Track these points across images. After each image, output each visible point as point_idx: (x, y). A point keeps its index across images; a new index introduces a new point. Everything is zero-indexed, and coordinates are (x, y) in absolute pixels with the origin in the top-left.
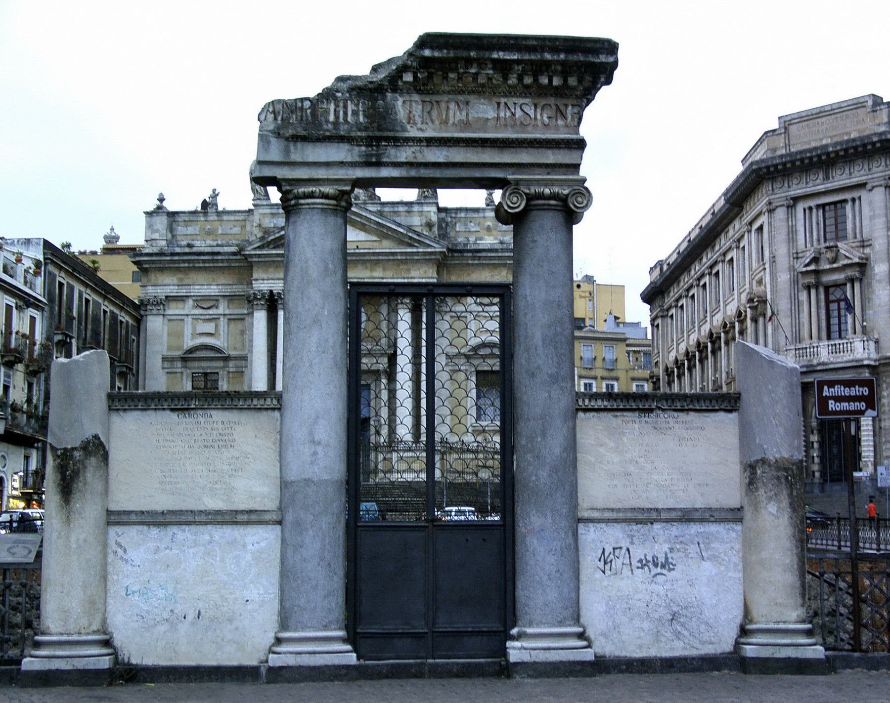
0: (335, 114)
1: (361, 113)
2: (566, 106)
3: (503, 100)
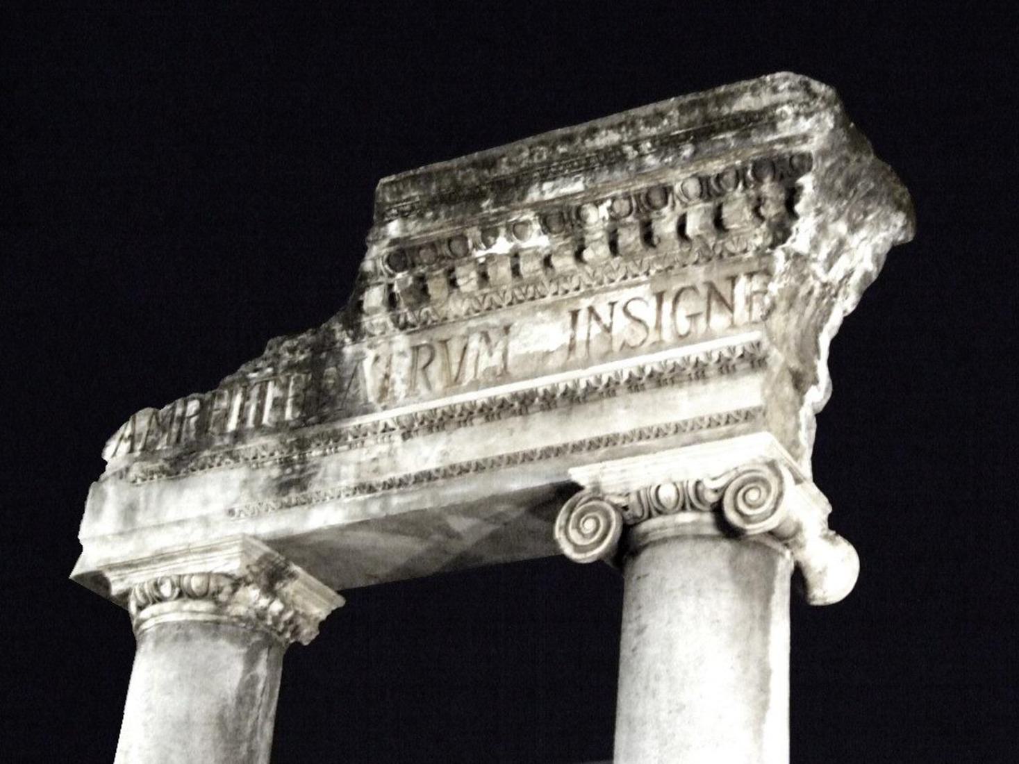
0: (239, 416)
1: (289, 401)
2: (733, 280)
3: (584, 303)
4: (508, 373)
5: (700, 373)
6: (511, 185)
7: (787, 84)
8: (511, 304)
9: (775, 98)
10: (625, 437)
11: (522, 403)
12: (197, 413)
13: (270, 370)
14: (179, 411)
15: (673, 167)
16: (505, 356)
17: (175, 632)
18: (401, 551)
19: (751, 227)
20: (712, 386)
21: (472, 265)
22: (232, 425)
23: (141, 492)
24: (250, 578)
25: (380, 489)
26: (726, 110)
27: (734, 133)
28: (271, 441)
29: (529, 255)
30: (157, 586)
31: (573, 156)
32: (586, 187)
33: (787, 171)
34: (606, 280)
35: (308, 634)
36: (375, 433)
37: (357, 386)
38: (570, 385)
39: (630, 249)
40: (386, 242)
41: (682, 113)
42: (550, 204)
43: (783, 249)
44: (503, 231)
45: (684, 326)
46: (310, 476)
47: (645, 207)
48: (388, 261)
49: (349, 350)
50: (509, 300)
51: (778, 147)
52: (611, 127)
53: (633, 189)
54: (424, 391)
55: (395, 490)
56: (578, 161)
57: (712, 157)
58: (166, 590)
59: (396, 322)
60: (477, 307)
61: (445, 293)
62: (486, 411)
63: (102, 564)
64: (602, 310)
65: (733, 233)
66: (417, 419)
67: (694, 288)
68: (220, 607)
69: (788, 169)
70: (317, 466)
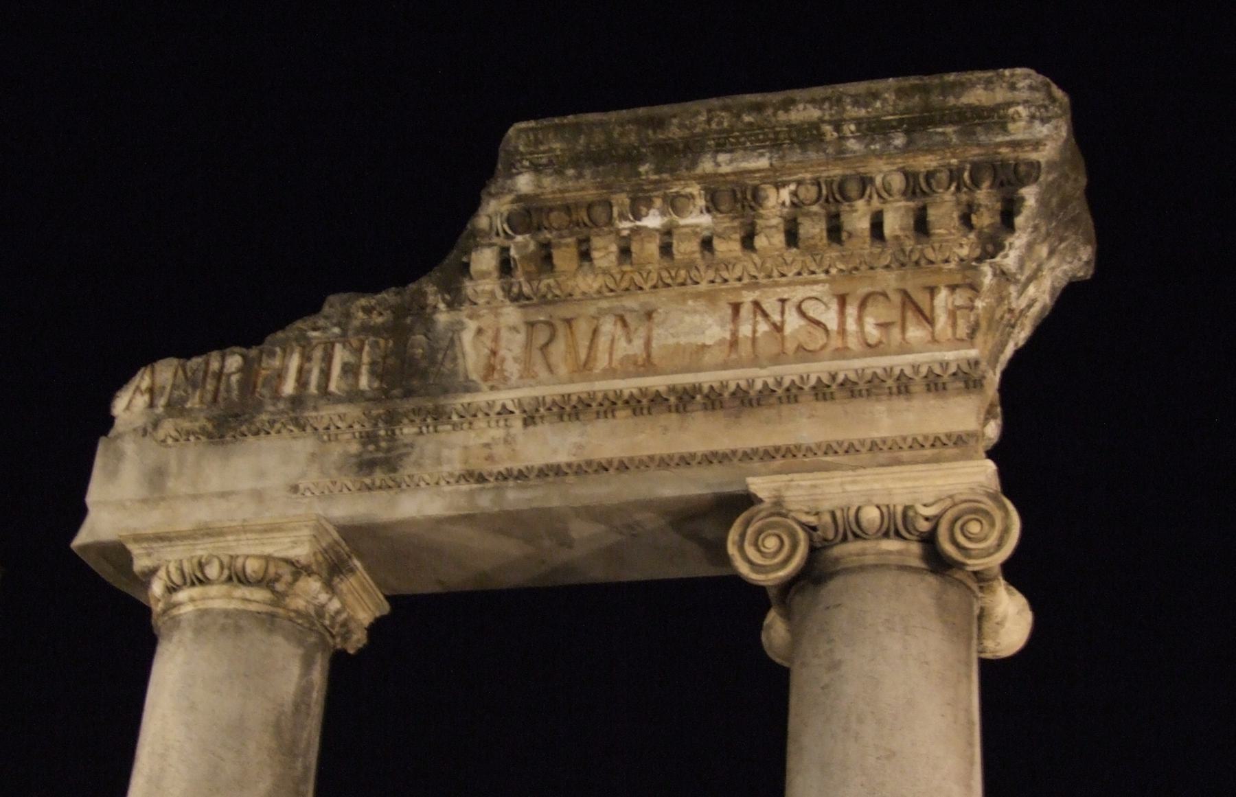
1: (364, 370)
2: (932, 291)
3: (748, 297)
4: (652, 364)
5: (903, 388)
6: (677, 151)
7: (1028, 82)
8: (655, 287)
9: (1009, 96)
10: (809, 449)
11: (680, 399)
12: (240, 370)
13: (336, 330)
14: (215, 365)
15: (879, 155)
16: (648, 343)
17: (222, 621)
18: (498, 558)
19: (958, 235)
20: (916, 403)
21: (612, 237)
22: (289, 388)
23: (172, 457)
24: (314, 567)
25: (492, 479)
26: (951, 101)
27: (955, 128)
28: (353, 411)
29: (686, 234)
30: (201, 566)
31: (761, 128)
32: (771, 165)
33: (1009, 178)
34: (775, 273)
35: (357, 640)
36: (487, 415)
37: (455, 359)
38: (743, 384)
39: (812, 242)
40: (510, 197)
41: (899, 97)
42: (722, 179)
43: (991, 265)
44: (658, 202)
45: (873, 333)
46: (400, 457)
47: (836, 197)
48: (509, 220)
49: (443, 317)
50: (654, 282)
51: (1003, 150)
52: (813, 101)
53: (825, 174)
54: (543, 374)
55: (511, 483)
56: (764, 134)
57: (929, 150)
58: (212, 571)
59: (507, 291)
60: (612, 286)
61: (574, 265)
62: (633, 403)
63: (124, 534)
64: (770, 305)
65: (934, 238)
66: (544, 404)
67: (884, 295)
68: (279, 597)
69: (1012, 176)
70: (412, 446)
